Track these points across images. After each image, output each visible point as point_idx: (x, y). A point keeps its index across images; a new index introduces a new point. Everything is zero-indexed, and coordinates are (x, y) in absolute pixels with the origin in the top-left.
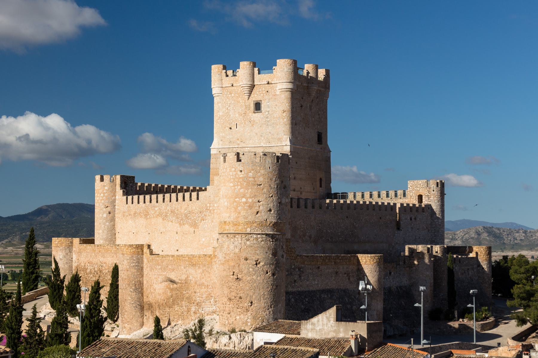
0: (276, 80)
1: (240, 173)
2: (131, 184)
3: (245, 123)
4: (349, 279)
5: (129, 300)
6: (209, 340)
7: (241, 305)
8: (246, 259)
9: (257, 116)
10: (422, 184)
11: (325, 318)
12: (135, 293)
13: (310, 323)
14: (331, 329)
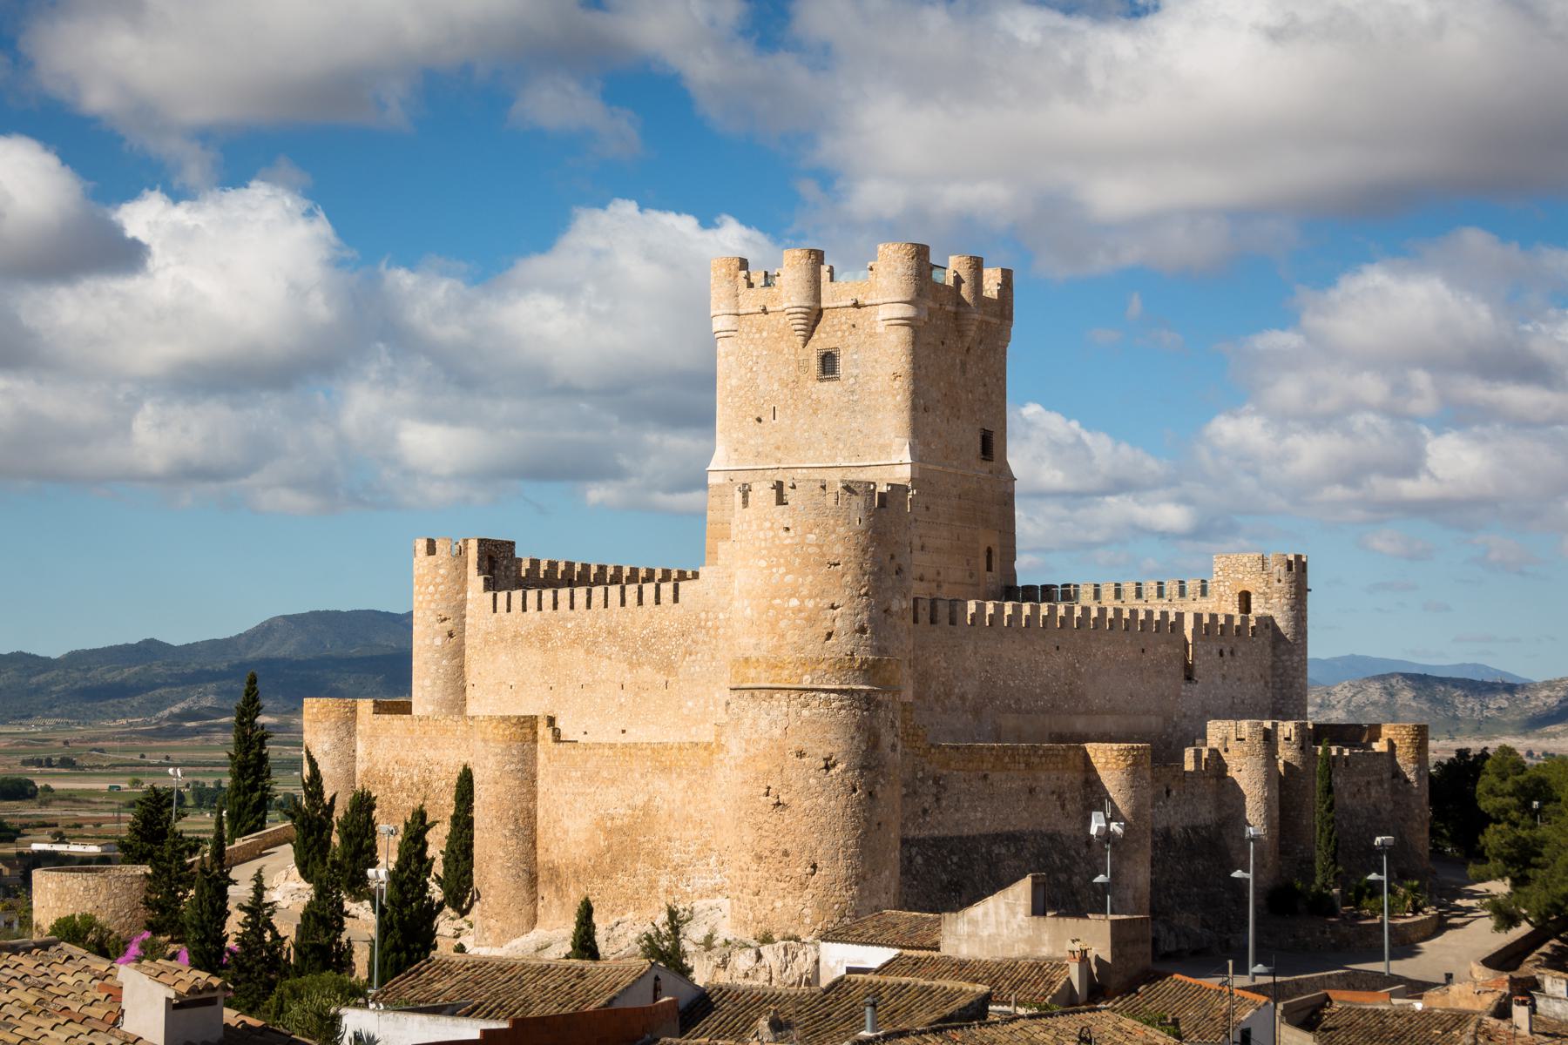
0: (874, 295)
1: (785, 534)
2: (505, 562)
4: (1063, 807)
5: (501, 858)
6: (706, 961)
7: (787, 872)
8: (801, 754)
9: (828, 390)
10: (1248, 565)
11: (1003, 906)
13: (966, 919)
14: (1020, 935)
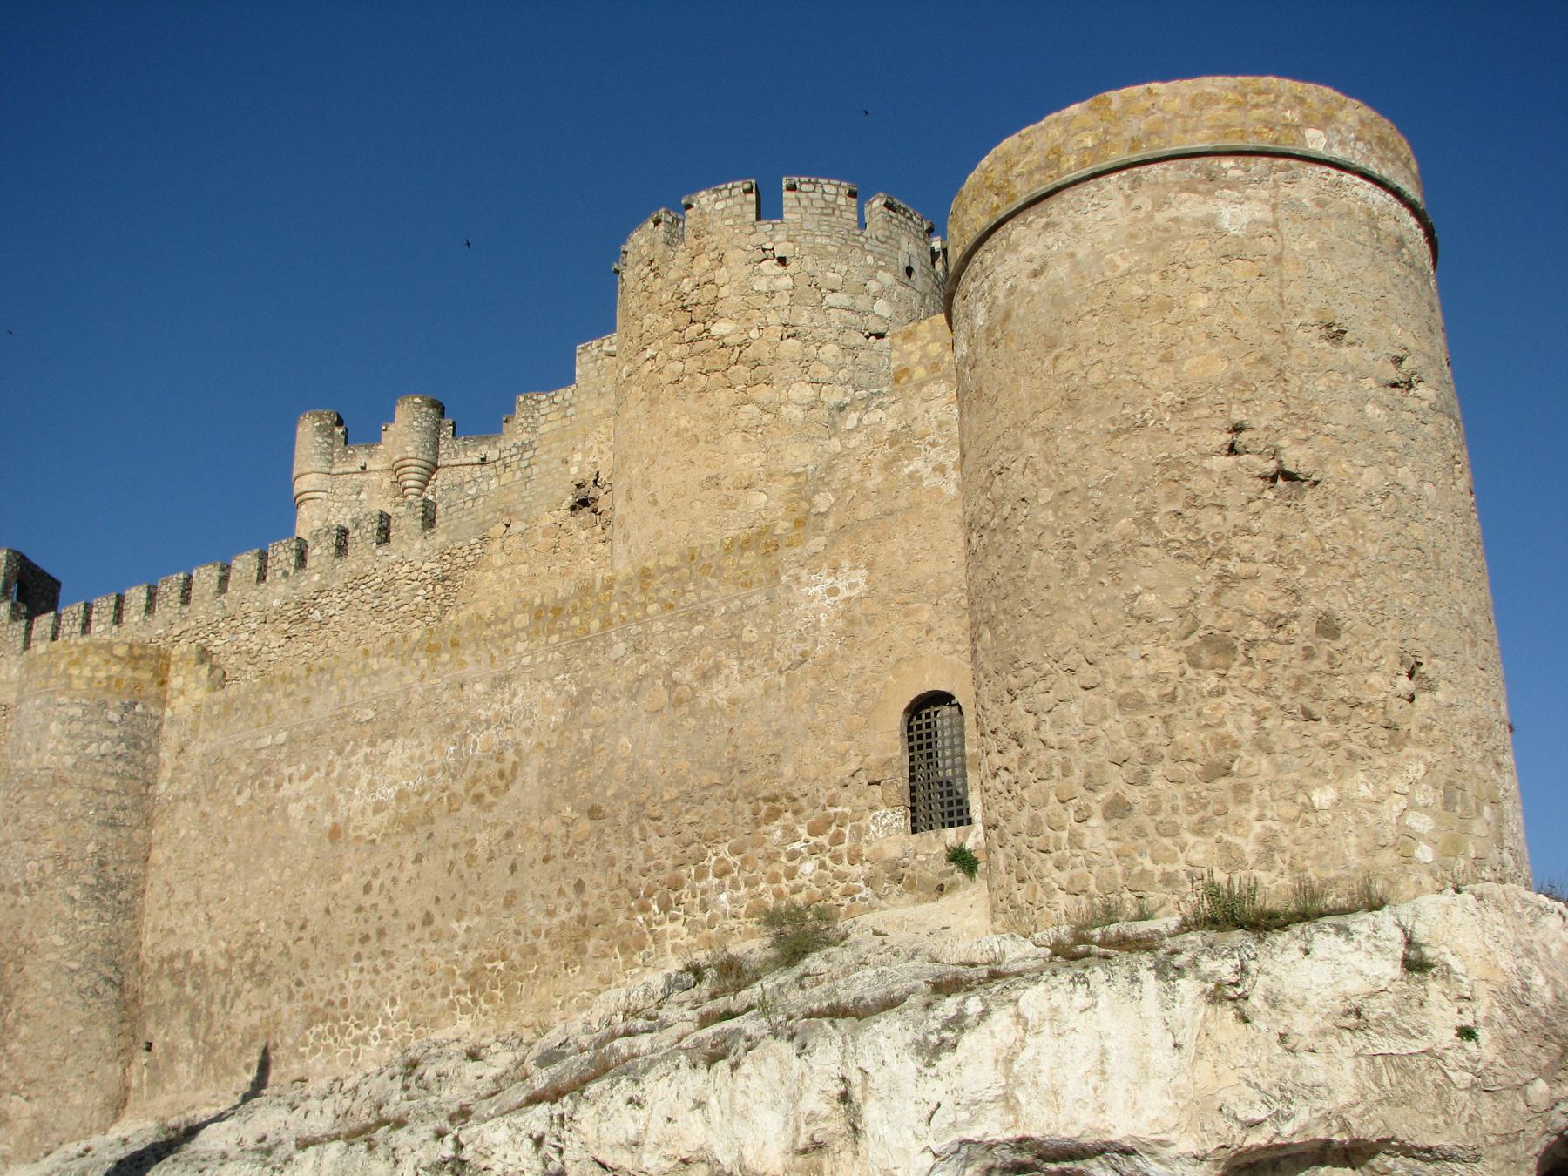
1: (780, 269)
5: (55, 948)
12: (92, 913)
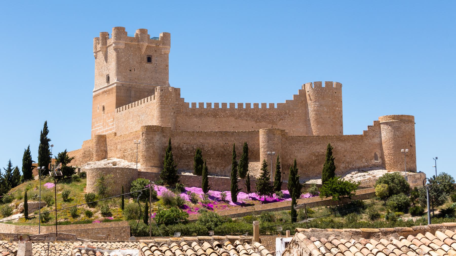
3: (141, 69)
9: (148, 65)
